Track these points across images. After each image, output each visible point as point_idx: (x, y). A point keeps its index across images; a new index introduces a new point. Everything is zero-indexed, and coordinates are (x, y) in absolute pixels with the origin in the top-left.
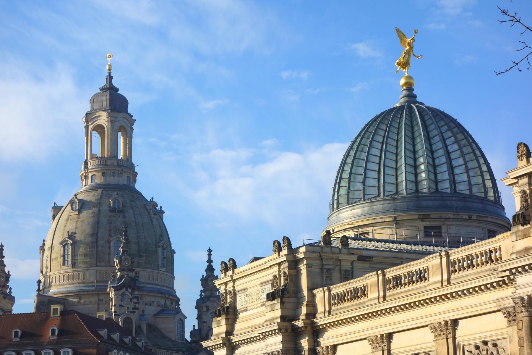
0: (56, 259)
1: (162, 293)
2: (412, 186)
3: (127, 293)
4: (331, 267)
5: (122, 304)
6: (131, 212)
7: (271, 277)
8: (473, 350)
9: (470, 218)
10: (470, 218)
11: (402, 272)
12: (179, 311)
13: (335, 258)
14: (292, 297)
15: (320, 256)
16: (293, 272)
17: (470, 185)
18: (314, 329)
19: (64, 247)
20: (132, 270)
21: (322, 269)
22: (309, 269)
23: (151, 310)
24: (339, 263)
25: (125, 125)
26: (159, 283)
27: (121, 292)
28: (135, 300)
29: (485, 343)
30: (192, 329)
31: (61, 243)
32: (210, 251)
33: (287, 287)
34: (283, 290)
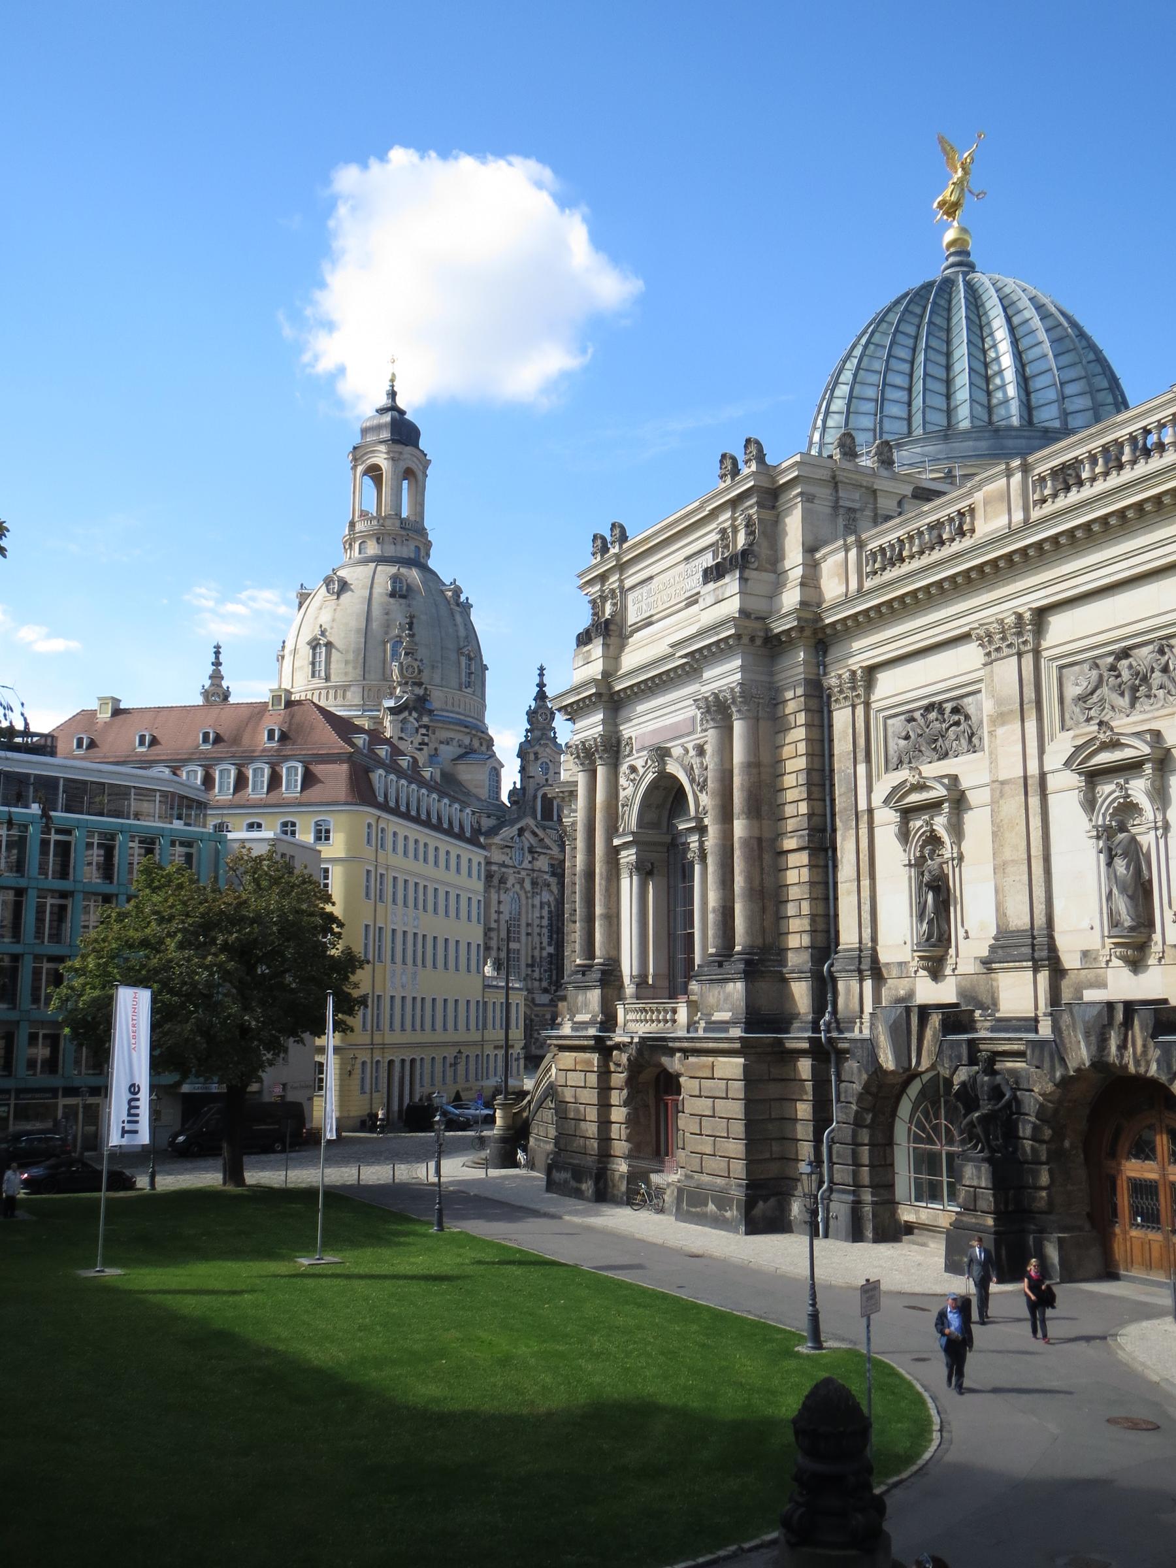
0: (301, 668)
1: (466, 727)
3: (411, 719)
4: (857, 505)
5: (403, 735)
7: (714, 537)
11: (1084, 450)
12: (493, 755)
13: (865, 484)
14: (766, 571)
15: (834, 477)
16: (768, 515)
18: (820, 636)
19: (314, 648)
20: (420, 684)
21: (836, 507)
22: (808, 505)
23: (448, 752)
24: (871, 501)
25: (414, 467)
26: (461, 710)
27: (401, 717)
28: (423, 731)
30: (511, 787)
31: (309, 643)
32: (542, 669)
33: (755, 548)
34: (744, 553)
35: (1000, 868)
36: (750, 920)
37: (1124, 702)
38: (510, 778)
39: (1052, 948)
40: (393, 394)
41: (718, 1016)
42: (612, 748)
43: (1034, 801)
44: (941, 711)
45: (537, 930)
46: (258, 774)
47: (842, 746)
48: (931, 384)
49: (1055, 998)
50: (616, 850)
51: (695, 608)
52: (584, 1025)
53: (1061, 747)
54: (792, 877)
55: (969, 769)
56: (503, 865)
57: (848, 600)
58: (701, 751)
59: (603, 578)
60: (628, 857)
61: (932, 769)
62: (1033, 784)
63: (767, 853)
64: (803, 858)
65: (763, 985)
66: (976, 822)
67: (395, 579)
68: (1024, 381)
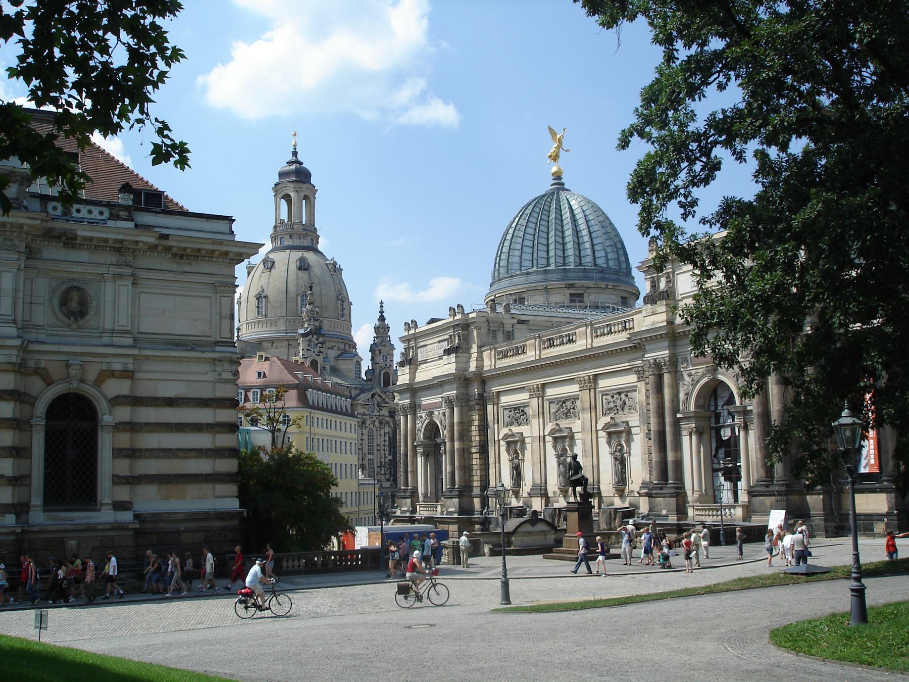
2: (561, 260)
7: (447, 337)
8: (609, 397)
9: (607, 286)
10: (607, 286)
12: (357, 355)
17: (607, 260)
19: (258, 299)
21: (489, 330)
23: (332, 354)
25: (308, 194)
29: (619, 393)
35: (533, 464)
36: (460, 477)
38: (366, 364)
39: (546, 490)
40: (295, 154)
41: (450, 510)
42: (414, 408)
43: (542, 444)
45: (382, 448)
47: (490, 418)
48: (540, 247)
49: (546, 505)
52: (405, 511)
54: (474, 462)
55: (525, 430)
56: (364, 414)
57: (491, 370)
58: (444, 415)
59: (409, 341)
60: (420, 450)
61: (516, 429)
63: (466, 453)
64: (477, 456)
65: (464, 499)
67: (302, 260)
68: (578, 244)
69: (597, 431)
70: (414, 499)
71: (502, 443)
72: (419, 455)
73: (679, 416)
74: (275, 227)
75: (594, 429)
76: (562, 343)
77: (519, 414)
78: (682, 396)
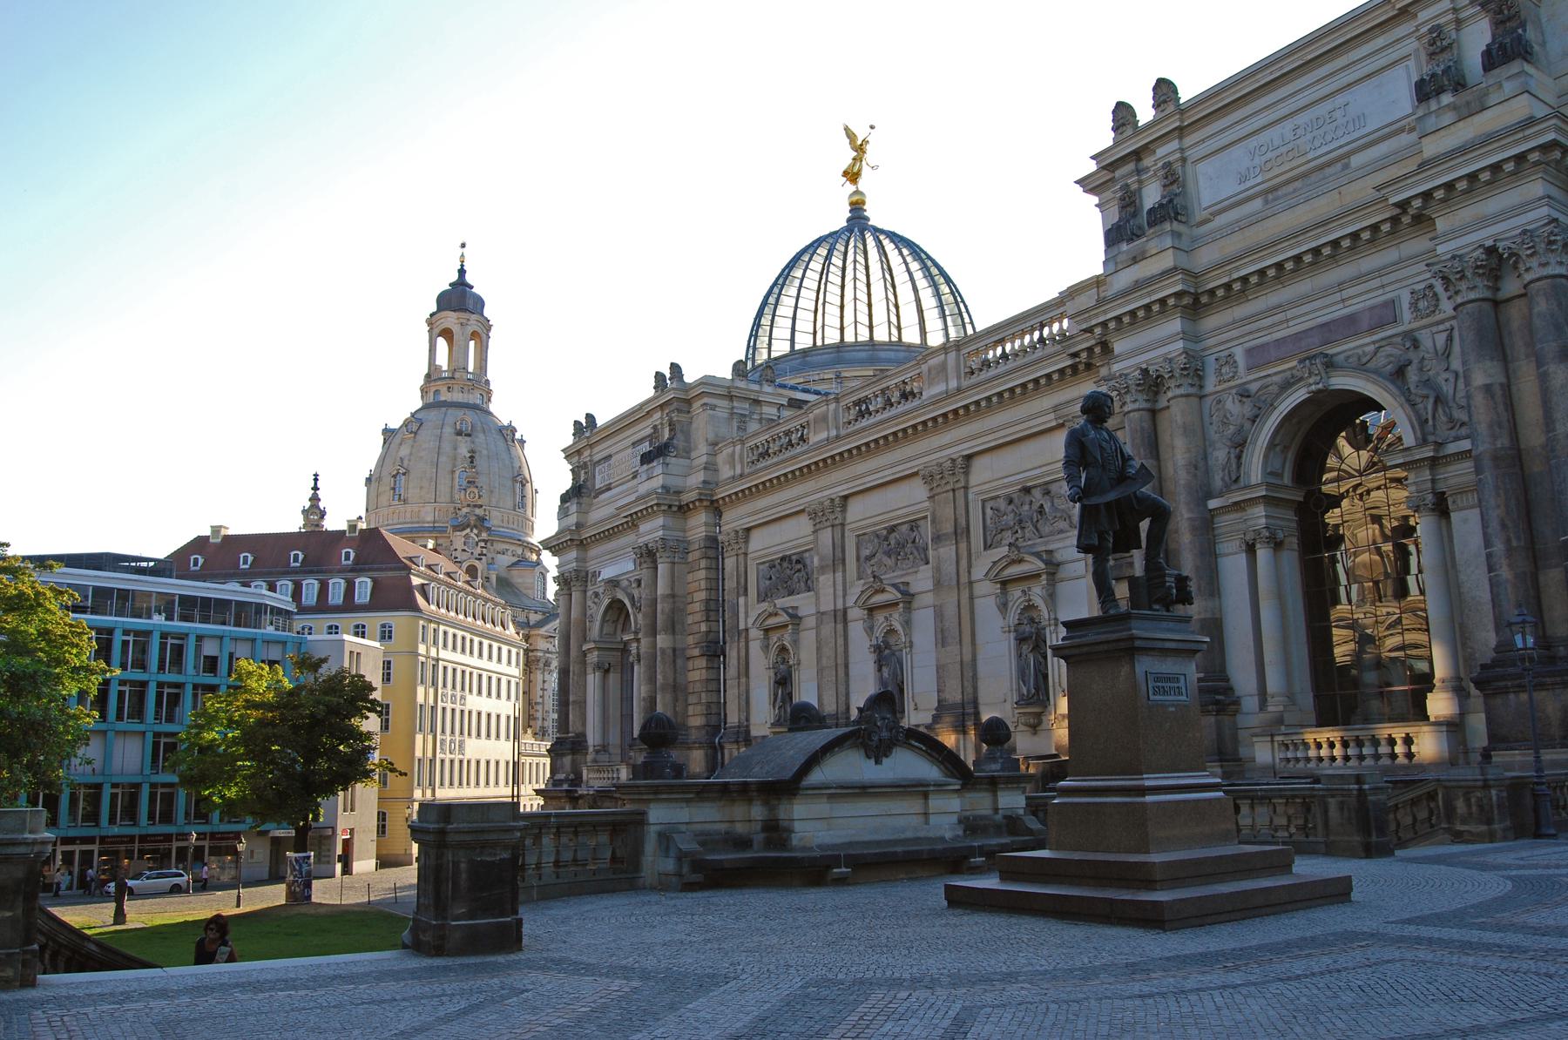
6: (481, 436)
7: (649, 431)
8: (1002, 504)
23: (506, 560)
29: (1027, 490)
35: (820, 671)
37: (890, 562)
40: (462, 272)
44: (790, 561)
46: (337, 587)
47: (730, 584)
50: (584, 654)
51: (635, 482)
53: (856, 590)
55: (803, 603)
58: (639, 582)
59: (579, 452)
61: (780, 602)
62: (840, 615)
66: (808, 638)
69: (971, 583)
70: (579, 757)
71: (755, 633)
72: (589, 670)
73: (1213, 504)
74: (428, 376)
75: (964, 579)
76: (889, 404)
77: (790, 572)
78: (1220, 455)
